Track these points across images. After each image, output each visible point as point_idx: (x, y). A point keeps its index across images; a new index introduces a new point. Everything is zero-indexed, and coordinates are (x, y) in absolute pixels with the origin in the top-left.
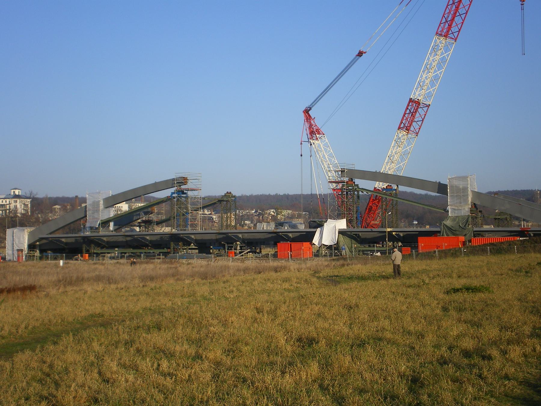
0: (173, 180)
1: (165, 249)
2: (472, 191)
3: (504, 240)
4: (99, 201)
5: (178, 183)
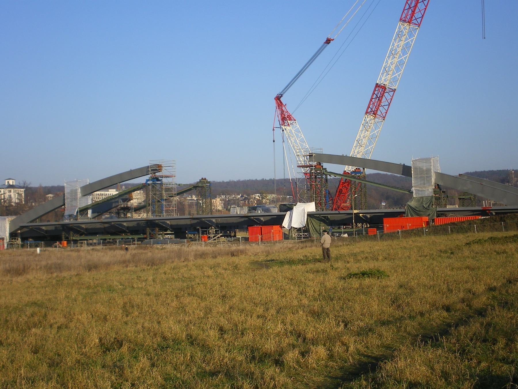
0: (148, 167)
1: (142, 235)
2: (435, 172)
4: (77, 190)
5: (152, 170)
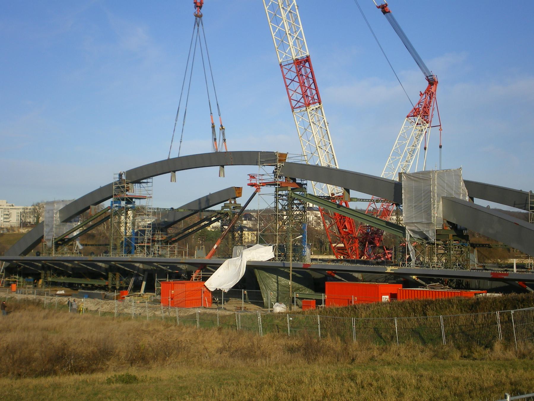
2: (443, 198)
3: (451, 295)
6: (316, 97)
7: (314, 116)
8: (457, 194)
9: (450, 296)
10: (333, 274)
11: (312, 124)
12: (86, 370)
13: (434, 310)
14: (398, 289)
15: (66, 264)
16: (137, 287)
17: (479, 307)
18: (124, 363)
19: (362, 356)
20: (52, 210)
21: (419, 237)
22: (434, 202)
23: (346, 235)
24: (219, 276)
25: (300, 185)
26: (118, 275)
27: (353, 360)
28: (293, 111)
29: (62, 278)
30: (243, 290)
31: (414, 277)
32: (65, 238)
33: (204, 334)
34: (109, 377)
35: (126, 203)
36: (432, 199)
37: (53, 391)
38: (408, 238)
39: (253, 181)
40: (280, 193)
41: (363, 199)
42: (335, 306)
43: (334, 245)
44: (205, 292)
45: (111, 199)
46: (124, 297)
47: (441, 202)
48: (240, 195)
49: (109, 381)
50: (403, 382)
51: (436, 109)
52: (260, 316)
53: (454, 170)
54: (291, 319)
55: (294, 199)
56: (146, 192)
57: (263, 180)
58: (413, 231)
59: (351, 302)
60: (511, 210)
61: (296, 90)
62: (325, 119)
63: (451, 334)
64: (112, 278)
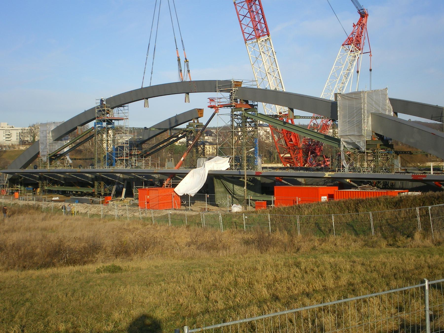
3: (379, 195)
6: (265, 30)
7: (264, 47)
8: (384, 110)
9: (378, 196)
10: (280, 180)
11: (262, 53)
12: (79, 262)
13: (364, 208)
14: (335, 190)
15: (58, 175)
16: (118, 194)
17: (402, 204)
18: (110, 256)
19: (305, 246)
20: (46, 131)
21: (352, 147)
22: (364, 117)
23: (292, 147)
24: (186, 183)
25: (252, 106)
26: (102, 183)
27: (298, 250)
28: (246, 43)
29: (56, 186)
30: (206, 194)
31: (348, 180)
32: (57, 153)
33: (175, 230)
34: (98, 268)
35: (107, 124)
36: (362, 115)
37: (52, 280)
38: (342, 148)
39: (213, 104)
40: (235, 113)
41: (305, 117)
42: (282, 206)
43: (282, 155)
44: (175, 197)
45: (95, 121)
46: (108, 202)
47: (370, 118)
48: (201, 115)
49: (98, 271)
50: (339, 268)
51: (367, 37)
52: (221, 215)
53: (381, 90)
54: (246, 217)
55: (247, 118)
56: (123, 115)
57: (221, 102)
58: (347, 143)
59: (296, 202)
60: (429, 122)
61: (248, 24)
62: (273, 49)
63: (379, 227)
64: (98, 186)
